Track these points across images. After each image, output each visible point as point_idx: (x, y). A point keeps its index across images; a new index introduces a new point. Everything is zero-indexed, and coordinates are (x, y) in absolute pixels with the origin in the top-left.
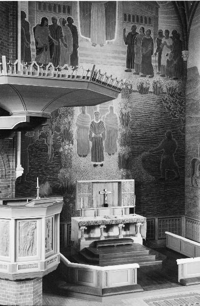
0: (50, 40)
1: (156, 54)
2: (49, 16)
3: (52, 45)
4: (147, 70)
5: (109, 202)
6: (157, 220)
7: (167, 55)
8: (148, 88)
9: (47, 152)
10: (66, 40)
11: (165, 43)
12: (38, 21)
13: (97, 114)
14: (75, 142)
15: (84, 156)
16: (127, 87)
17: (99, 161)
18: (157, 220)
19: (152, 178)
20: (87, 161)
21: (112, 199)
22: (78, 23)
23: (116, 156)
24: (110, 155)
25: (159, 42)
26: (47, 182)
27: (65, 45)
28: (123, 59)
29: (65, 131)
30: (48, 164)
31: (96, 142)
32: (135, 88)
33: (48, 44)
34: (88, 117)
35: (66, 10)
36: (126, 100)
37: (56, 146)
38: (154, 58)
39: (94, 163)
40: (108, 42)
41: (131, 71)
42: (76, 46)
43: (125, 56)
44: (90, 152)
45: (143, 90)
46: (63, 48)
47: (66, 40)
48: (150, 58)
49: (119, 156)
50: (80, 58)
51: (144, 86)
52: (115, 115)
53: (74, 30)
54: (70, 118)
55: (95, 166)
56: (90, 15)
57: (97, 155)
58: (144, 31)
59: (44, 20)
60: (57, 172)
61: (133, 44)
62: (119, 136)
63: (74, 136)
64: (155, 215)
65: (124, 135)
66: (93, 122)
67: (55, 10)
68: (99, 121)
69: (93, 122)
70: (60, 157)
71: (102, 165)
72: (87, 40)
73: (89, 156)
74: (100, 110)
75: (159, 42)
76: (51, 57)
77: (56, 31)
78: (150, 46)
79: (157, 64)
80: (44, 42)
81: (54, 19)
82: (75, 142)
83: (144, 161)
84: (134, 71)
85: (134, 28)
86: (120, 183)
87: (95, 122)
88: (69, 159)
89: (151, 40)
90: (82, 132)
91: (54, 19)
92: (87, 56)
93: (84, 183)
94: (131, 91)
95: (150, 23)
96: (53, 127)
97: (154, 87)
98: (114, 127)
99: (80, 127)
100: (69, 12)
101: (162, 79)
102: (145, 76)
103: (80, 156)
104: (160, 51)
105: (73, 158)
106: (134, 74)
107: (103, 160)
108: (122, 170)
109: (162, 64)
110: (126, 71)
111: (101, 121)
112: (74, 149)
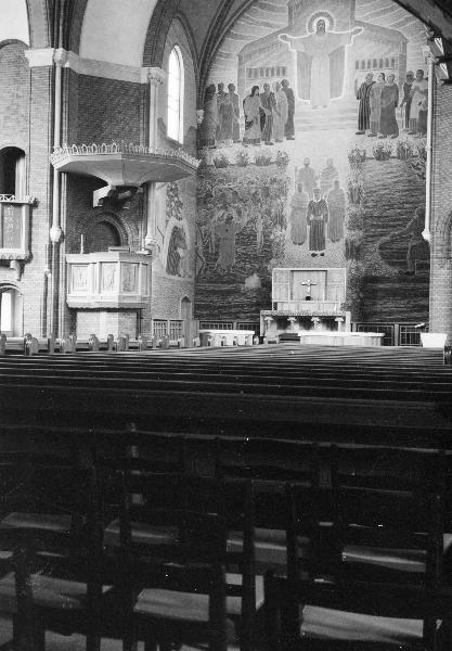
0: (261, 110)
1: (402, 106)
4: (390, 128)
7: (420, 104)
11: (417, 88)
12: (248, 90)
13: (317, 191)
14: (289, 226)
15: (300, 244)
16: (358, 154)
18: (397, 326)
19: (395, 271)
20: (305, 250)
22: (294, 85)
23: (342, 242)
24: (333, 241)
25: (407, 88)
27: (279, 115)
33: (259, 117)
37: (266, 236)
38: (399, 112)
42: (291, 113)
43: (357, 115)
44: (308, 241)
45: (382, 156)
46: (276, 119)
49: (347, 244)
53: (290, 95)
54: (283, 198)
55: (314, 255)
57: (317, 242)
59: (255, 88)
60: (267, 261)
65: (354, 216)
71: (323, 255)
75: (407, 88)
77: (268, 100)
78: (393, 95)
80: (254, 115)
82: (289, 226)
84: (368, 132)
85: (371, 76)
89: (395, 89)
91: (266, 85)
93: (282, 272)
94: (364, 159)
95: (393, 65)
96: (263, 210)
99: (295, 209)
100: (284, 72)
101: (411, 139)
104: (408, 100)
106: (372, 136)
109: (412, 116)
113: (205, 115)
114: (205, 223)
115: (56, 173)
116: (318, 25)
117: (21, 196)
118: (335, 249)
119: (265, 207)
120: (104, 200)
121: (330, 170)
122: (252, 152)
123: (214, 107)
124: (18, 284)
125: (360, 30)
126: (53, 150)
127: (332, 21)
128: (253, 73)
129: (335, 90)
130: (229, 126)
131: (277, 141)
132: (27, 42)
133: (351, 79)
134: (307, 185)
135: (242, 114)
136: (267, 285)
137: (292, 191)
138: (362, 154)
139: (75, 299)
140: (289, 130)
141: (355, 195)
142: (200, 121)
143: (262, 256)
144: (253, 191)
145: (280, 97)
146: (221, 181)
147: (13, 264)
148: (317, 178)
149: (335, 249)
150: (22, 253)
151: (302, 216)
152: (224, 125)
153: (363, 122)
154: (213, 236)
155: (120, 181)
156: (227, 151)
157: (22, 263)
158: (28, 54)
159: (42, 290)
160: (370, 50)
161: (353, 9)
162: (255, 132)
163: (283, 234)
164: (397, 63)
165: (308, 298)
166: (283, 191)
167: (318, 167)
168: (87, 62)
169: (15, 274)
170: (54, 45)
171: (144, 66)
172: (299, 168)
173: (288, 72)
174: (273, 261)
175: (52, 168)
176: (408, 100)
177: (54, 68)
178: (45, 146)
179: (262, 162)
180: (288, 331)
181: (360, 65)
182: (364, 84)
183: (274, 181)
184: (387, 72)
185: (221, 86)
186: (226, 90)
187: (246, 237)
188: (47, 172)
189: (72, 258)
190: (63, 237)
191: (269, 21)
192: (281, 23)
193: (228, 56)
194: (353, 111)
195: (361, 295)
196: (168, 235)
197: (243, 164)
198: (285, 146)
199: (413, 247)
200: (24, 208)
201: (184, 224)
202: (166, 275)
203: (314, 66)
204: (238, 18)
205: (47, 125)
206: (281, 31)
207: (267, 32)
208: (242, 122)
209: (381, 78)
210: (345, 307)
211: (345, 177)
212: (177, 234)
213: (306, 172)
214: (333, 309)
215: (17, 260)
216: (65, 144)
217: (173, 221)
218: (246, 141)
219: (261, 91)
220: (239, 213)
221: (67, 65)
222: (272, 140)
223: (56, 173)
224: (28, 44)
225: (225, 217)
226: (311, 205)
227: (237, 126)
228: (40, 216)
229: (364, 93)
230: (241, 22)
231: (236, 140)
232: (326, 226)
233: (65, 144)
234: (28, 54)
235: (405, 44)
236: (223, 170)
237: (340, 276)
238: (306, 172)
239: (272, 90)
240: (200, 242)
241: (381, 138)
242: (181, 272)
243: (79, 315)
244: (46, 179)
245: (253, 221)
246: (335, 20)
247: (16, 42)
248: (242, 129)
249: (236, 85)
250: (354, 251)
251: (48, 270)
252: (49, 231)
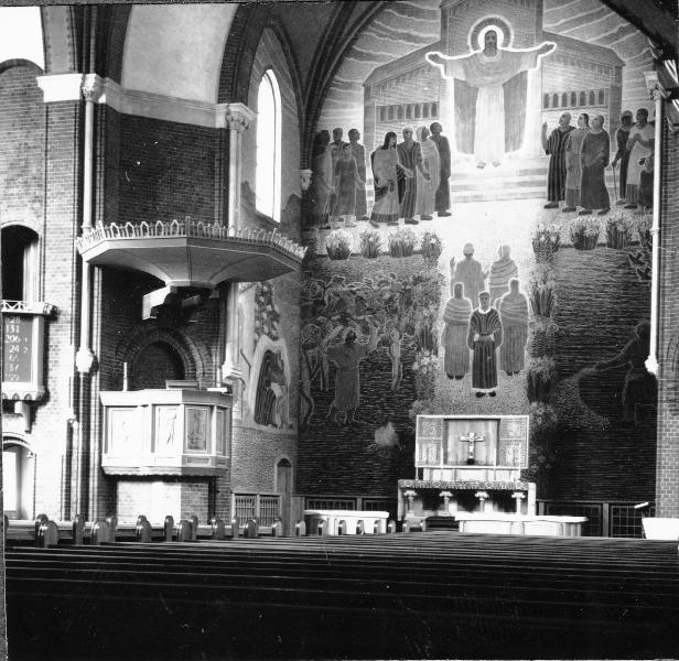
1: (614, 164)
2: (398, 128)
3: (401, 182)
4: (595, 198)
5: (481, 457)
6: (606, 506)
7: (642, 162)
8: (596, 237)
9: (390, 371)
10: (427, 168)
11: (637, 137)
12: (379, 140)
13: (484, 297)
14: (442, 352)
15: (459, 378)
16: (548, 238)
17: (488, 387)
18: (606, 506)
19: (603, 421)
20: (464, 388)
21: (487, 453)
22: (449, 131)
23: (523, 376)
24: (510, 374)
26: (390, 425)
27: (427, 176)
28: (540, 184)
29: (423, 333)
30: (392, 393)
31: (481, 349)
32: (566, 239)
34: (467, 304)
35: (430, 111)
36: (546, 266)
37: (407, 361)
38: (611, 175)
39: (478, 390)
40: (510, 157)
41: (557, 206)
42: (445, 174)
43: (545, 178)
45: (582, 241)
47: (427, 168)
48: (601, 172)
49: (530, 379)
50: (453, 195)
51: (588, 232)
52: (522, 295)
53: (443, 145)
55: (479, 395)
56: (474, 112)
57: (484, 376)
58: (587, 122)
59: (391, 136)
61: (563, 151)
62: (529, 339)
63: (439, 341)
64: (606, 497)
65: (540, 335)
66: (476, 313)
67: (409, 116)
68: (489, 310)
69: (476, 313)
70: (412, 381)
71: (493, 394)
72: (467, 160)
73: (469, 377)
74: (491, 289)
76: (400, 202)
77: (410, 153)
79: (618, 185)
81: (407, 133)
82: (442, 352)
83: (583, 383)
84: (563, 204)
85: (566, 118)
86: (498, 420)
87: (481, 312)
88: (429, 379)
89: (604, 138)
90: (457, 334)
91: (407, 133)
92: (465, 188)
93: (430, 420)
94: (557, 247)
96: (403, 324)
97: (609, 232)
98: (520, 320)
99: (451, 324)
102: (591, 213)
103: (451, 377)
104: (624, 155)
105: (437, 381)
106: (564, 211)
107: (495, 385)
108: (534, 404)
109: (628, 182)
110: (546, 207)
111: (492, 310)
112: (439, 365)
113: (313, 178)
114: (313, 346)
115: (85, 267)
116: (487, 37)
117: (31, 303)
118: (510, 386)
119: (405, 320)
120: (157, 310)
121: (504, 264)
122: (385, 235)
123: (328, 164)
124: (27, 437)
125: (551, 47)
126: (80, 232)
127: (507, 35)
128: (388, 113)
129: (512, 140)
130: (351, 193)
131: (426, 218)
132: (41, 65)
133: (538, 121)
134: (470, 286)
135: (369, 175)
136: (407, 440)
137: (447, 296)
138: (553, 239)
139: (114, 462)
140: (442, 204)
141: (542, 303)
142: (306, 185)
143: (399, 395)
144: (387, 296)
145: (427, 151)
146: (339, 281)
147: (18, 407)
148: (485, 277)
149: (510, 386)
150: (32, 389)
151: (462, 336)
152: (343, 193)
153: (556, 189)
154: (325, 363)
155: (183, 280)
156: (350, 234)
158: (43, 82)
159: (63, 451)
160: (562, 79)
161: (540, 13)
162: (390, 203)
163: (434, 362)
164: (608, 100)
165: (471, 462)
166: (434, 298)
167: (486, 258)
168: (134, 95)
169: (22, 423)
170: (82, 68)
171: (220, 101)
172: (457, 261)
173: (441, 111)
174: (416, 404)
175: (79, 259)
176: (624, 155)
177: (83, 103)
178: (68, 222)
179: (401, 250)
180: (441, 513)
181: (551, 101)
182: (556, 132)
183: (418, 280)
184: (593, 114)
185: (338, 133)
186: (346, 139)
187: (376, 365)
188: (69, 266)
189: (109, 397)
190: (95, 367)
191: (414, 33)
192: (432, 35)
193: (349, 86)
194: (539, 172)
195: (552, 458)
196: (257, 362)
197: (371, 252)
198: (436, 225)
199: (630, 382)
200: (36, 321)
201: (281, 346)
202: (256, 426)
203: (481, 103)
204: (364, 28)
205: (71, 194)
206: (429, 48)
207: (409, 48)
208: (370, 188)
209: (583, 121)
210: (527, 476)
211: (526, 276)
212: (270, 361)
213: (468, 267)
214: (508, 478)
215: (25, 402)
216: (100, 223)
217: (265, 342)
218: (376, 219)
219: (400, 140)
220: (366, 330)
221: (102, 100)
222: (417, 217)
223: (85, 267)
224: (43, 67)
225: (344, 337)
226: (476, 317)
227: (362, 194)
228: (61, 335)
229: (557, 144)
230: (370, 33)
231: (361, 217)
232: (498, 350)
233: (100, 223)
234: (43, 82)
235: (619, 69)
236: (341, 263)
237: (519, 426)
238: (468, 267)
239: (415, 138)
240: (306, 373)
241: (580, 214)
242: (277, 420)
243: (123, 488)
244: (70, 276)
245: (386, 342)
246: (512, 32)
247: (23, 63)
248: (370, 199)
249: (361, 131)
250: (539, 389)
251: (74, 417)
252: (72, 357)
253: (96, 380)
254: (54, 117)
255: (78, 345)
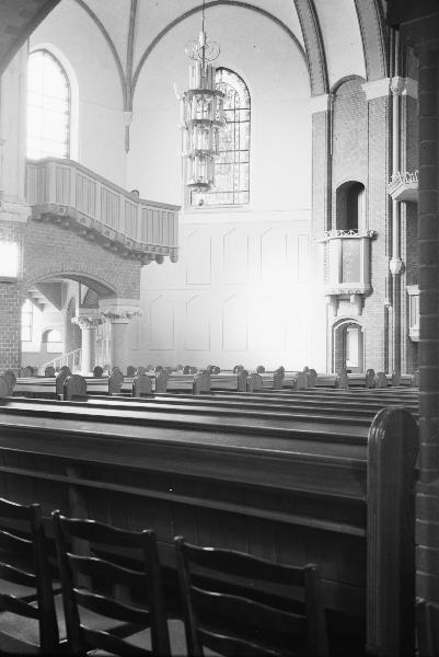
115: (395, 203)
117: (363, 231)
124: (359, 318)
147: (352, 298)
150: (361, 286)
157: (362, 298)
158: (365, 87)
159: (383, 325)
170: (390, 74)
177: (391, 97)
190: (403, 268)
221: (404, 93)
223: (395, 203)
224: (364, 76)
228: (379, 247)
234: (365, 87)
244: (384, 211)
247: (353, 77)
253: (404, 278)
254: (372, 109)
255: (391, 256)
